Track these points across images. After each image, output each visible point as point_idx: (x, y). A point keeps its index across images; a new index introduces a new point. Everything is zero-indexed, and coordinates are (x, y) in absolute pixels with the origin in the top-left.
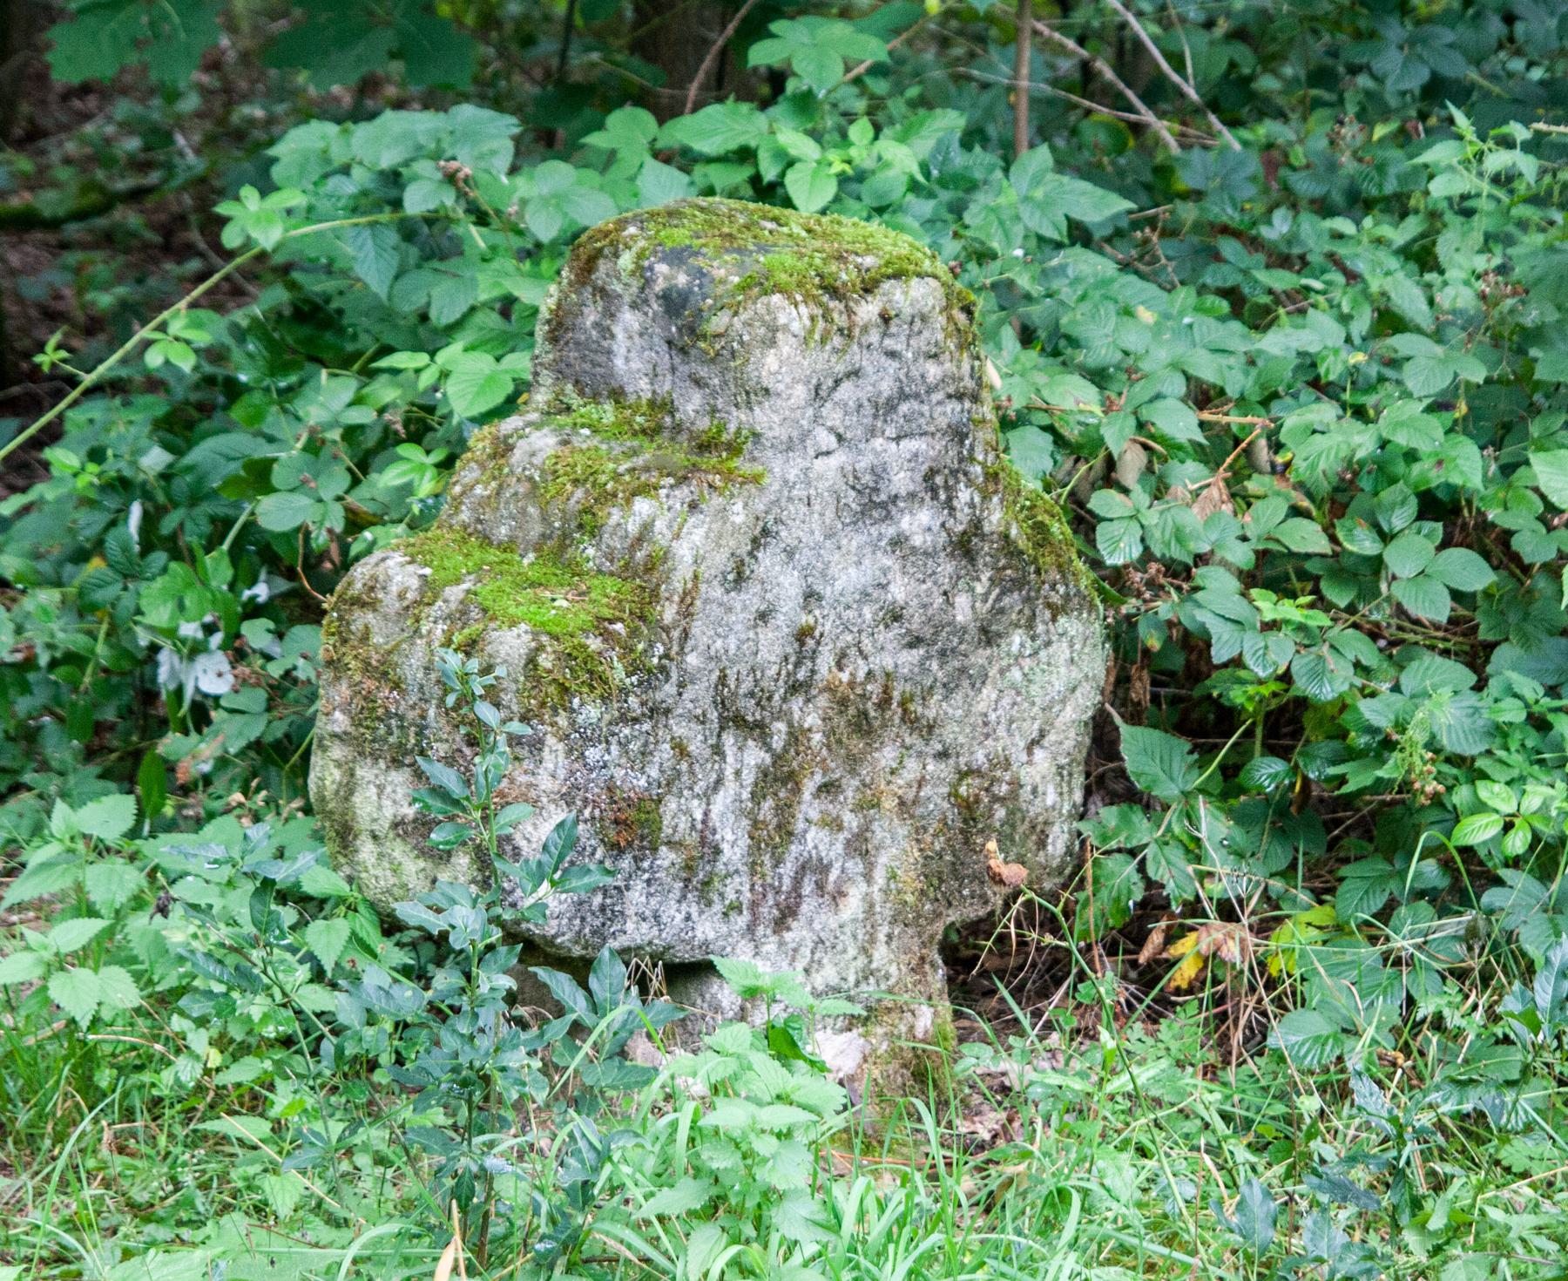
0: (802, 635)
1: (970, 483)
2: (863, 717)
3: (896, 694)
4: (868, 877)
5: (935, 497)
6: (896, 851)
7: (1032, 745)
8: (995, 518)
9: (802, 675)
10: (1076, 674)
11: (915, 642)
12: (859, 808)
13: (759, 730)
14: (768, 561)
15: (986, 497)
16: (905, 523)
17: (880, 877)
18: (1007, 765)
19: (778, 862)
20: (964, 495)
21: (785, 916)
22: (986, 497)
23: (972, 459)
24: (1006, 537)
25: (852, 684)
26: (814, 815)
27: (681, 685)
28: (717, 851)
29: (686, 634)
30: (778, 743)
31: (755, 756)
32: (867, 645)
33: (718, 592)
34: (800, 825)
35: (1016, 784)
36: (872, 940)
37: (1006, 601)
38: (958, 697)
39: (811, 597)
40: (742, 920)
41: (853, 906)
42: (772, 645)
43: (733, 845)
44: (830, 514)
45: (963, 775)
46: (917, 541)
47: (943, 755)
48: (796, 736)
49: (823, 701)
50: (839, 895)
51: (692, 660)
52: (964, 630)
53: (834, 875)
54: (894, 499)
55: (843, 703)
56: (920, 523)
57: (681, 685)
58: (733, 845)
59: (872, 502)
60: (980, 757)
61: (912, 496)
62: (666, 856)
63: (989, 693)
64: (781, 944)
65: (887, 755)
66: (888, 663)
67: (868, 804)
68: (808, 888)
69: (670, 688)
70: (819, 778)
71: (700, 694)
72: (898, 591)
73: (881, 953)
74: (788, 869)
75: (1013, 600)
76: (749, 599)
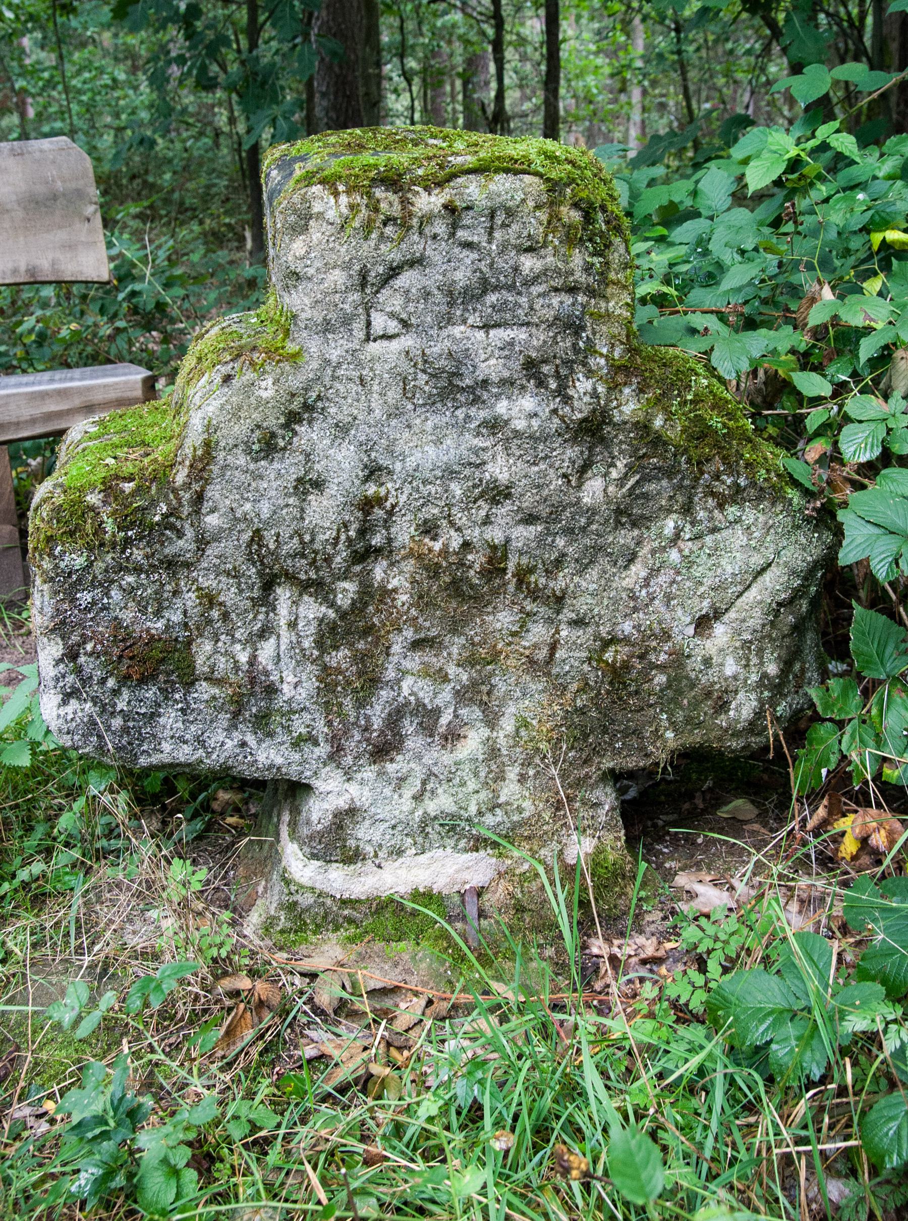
0: (367, 505)
1: (589, 374)
2: (462, 587)
3: (511, 566)
4: (491, 722)
5: (541, 383)
6: (525, 705)
7: (703, 624)
8: (629, 407)
9: (377, 540)
10: (757, 560)
11: (530, 519)
12: (470, 662)
13: (318, 588)
14: (309, 435)
15: (614, 387)
16: (502, 407)
17: (508, 725)
18: (666, 635)
19: (360, 704)
20: (583, 385)
21: (383, 750)
22: (614, 387)
23: (591, 349)
24: (643, 427)
25: (445, 552)
26: (407, 664)
27: (202, 542)
28: (271, 690)
29: (199, 498)
30: (343, 601)
31: (312, 610)
32: (461, 518)
33: (242, 460)
34: (391, 674)
35: (679, 658)
36: (501, 777)
37: (652, 487)
38: (594, 573)
39: (373, 472)
40: (323, 750)
41: (472, 743)
42: (325, 513)
43: (296, 685)
44: (393, 395)
45: (607, 644)
46: (520, 424)
47: (579, 623)
48: (369, 594)
49: (409, 566)
50: (452, 737)
51: (212, 521)
52: (592, 512)
53: (445, 720)
54: (485, 383)
55: (434, 571)
56: (522, 408)
57: (202, 542)
58: (296, 685)
59: (452, 385)
60: (627, 627)
61: (507, 383)
62: (204, 690)
63: (638, 570)
64: (381, 774)
65: (504, 619)
66: (496, 535)
67: (483, 659)
68: (409, 726)
69: (184, 545)
70: (409, 634)
71: (229, 550)
72: (500, 469)
73: (510, 790)
74: (377, 713)
75: (661, 487)
76: (287, 468)
